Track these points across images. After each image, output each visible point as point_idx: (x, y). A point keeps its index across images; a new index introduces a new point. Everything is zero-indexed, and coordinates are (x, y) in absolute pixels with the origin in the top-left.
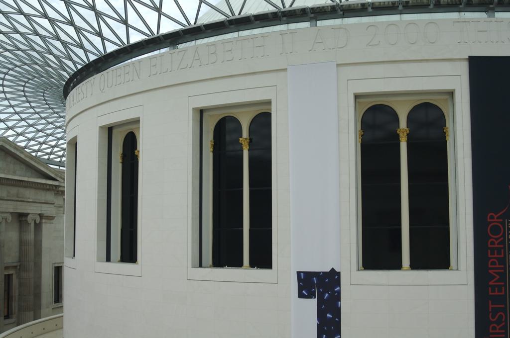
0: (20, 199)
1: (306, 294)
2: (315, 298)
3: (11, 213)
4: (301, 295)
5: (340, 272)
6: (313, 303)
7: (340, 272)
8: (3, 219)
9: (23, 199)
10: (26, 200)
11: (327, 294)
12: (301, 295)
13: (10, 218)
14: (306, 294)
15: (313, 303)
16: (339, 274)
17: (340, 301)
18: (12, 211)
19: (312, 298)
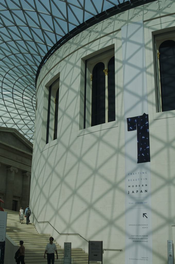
0: (23, 163)
1: (132, 129)
2: (136, 130)
3: (18, 169)
4: (129, 130)
5: (148, 115)
6: (135, 132)
7: (148, 115)
8: (13, 170)
9: (24, 163)
10: (26, 164)
11: (142, 127)
12: (129, 130)
13: (17, 171)
14: (132, 129)
15: (135, 132)
16: (148, 115)
17: (149, 129)
18: (18, 167)
19: (134, 130)
